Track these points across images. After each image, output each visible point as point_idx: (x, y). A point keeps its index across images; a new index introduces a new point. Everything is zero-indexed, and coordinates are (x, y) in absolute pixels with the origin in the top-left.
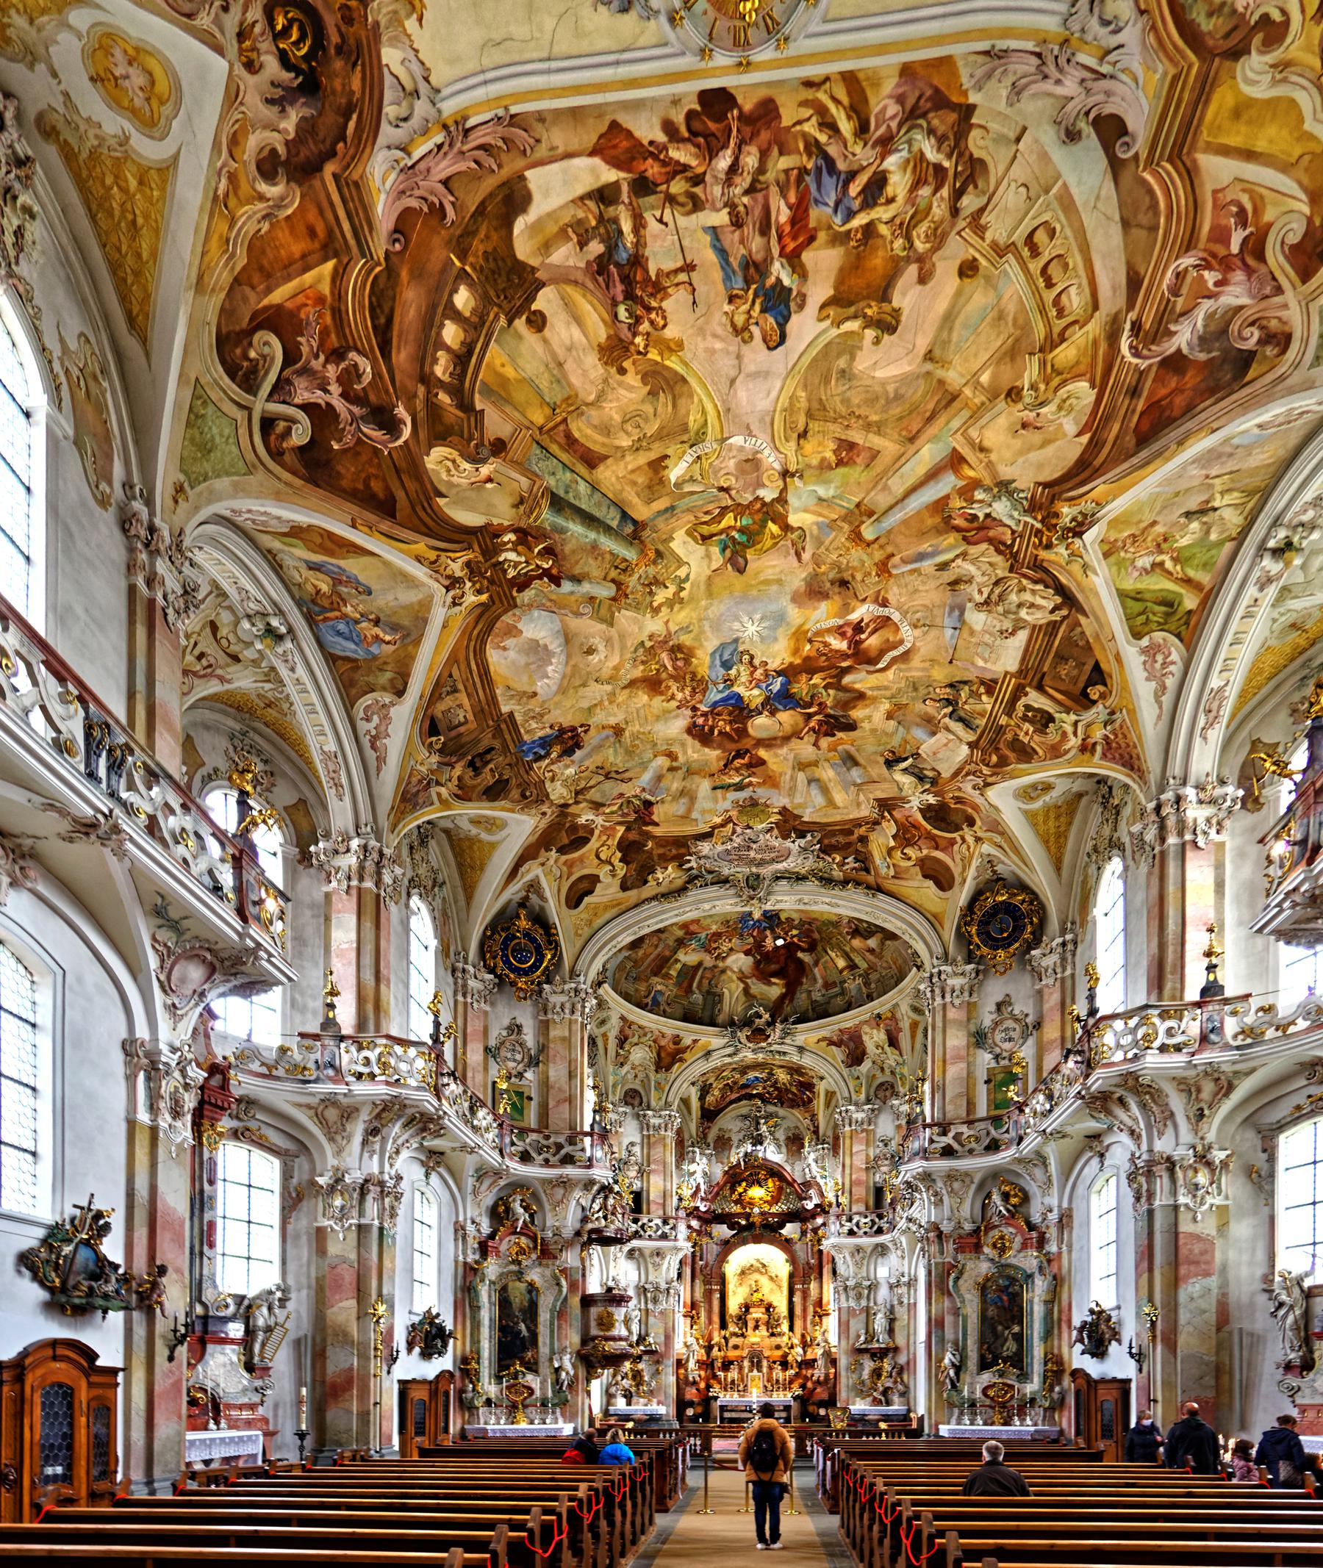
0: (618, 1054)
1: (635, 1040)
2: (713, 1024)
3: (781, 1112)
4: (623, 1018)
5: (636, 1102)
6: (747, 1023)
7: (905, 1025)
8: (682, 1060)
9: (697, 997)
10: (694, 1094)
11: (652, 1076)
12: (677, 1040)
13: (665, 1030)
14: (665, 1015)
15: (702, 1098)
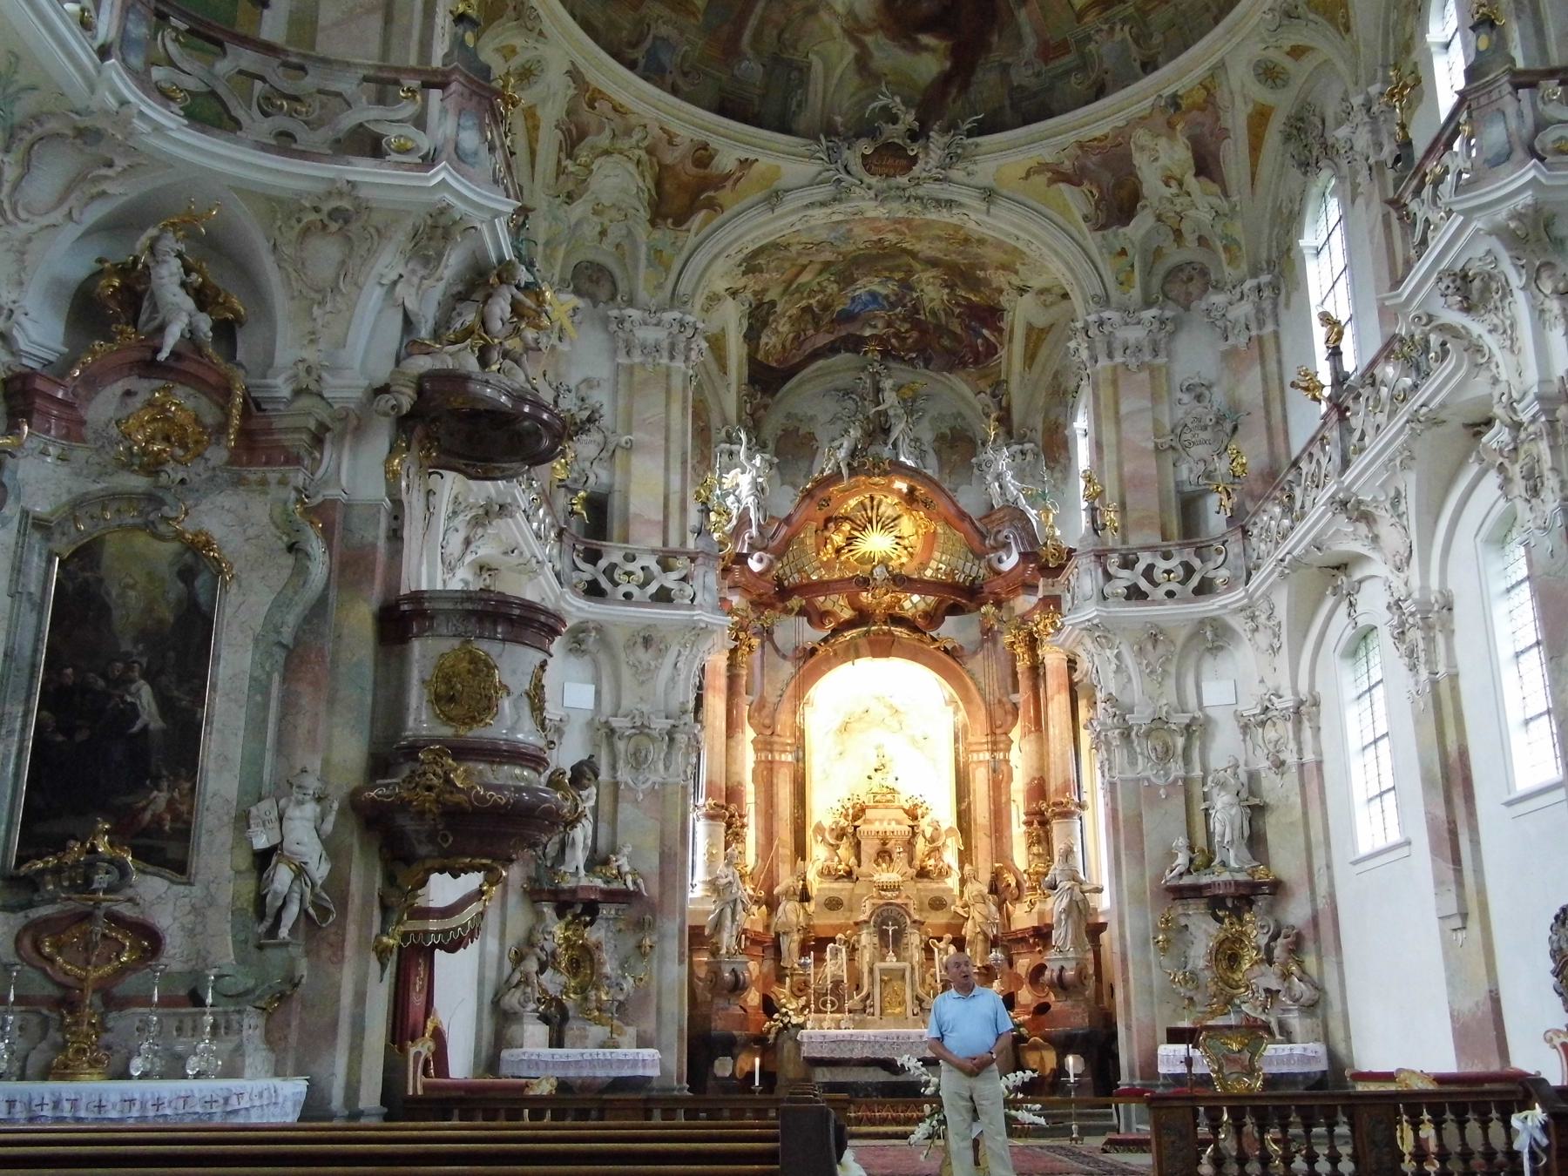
0: (560, 171)
1: (604, 141)
2: (784, 127)
3: (922, 378)
4: (574, 74)
5: (603, 292)
6: (865, 129)
7: (1237, 120)
8: (713, 206)
9: (751, 68)
10: (732, 319)
11: (642, 232)
12: (703, 155)
13: (675, 127)
14: (674, 91)
15: (752, 336)
